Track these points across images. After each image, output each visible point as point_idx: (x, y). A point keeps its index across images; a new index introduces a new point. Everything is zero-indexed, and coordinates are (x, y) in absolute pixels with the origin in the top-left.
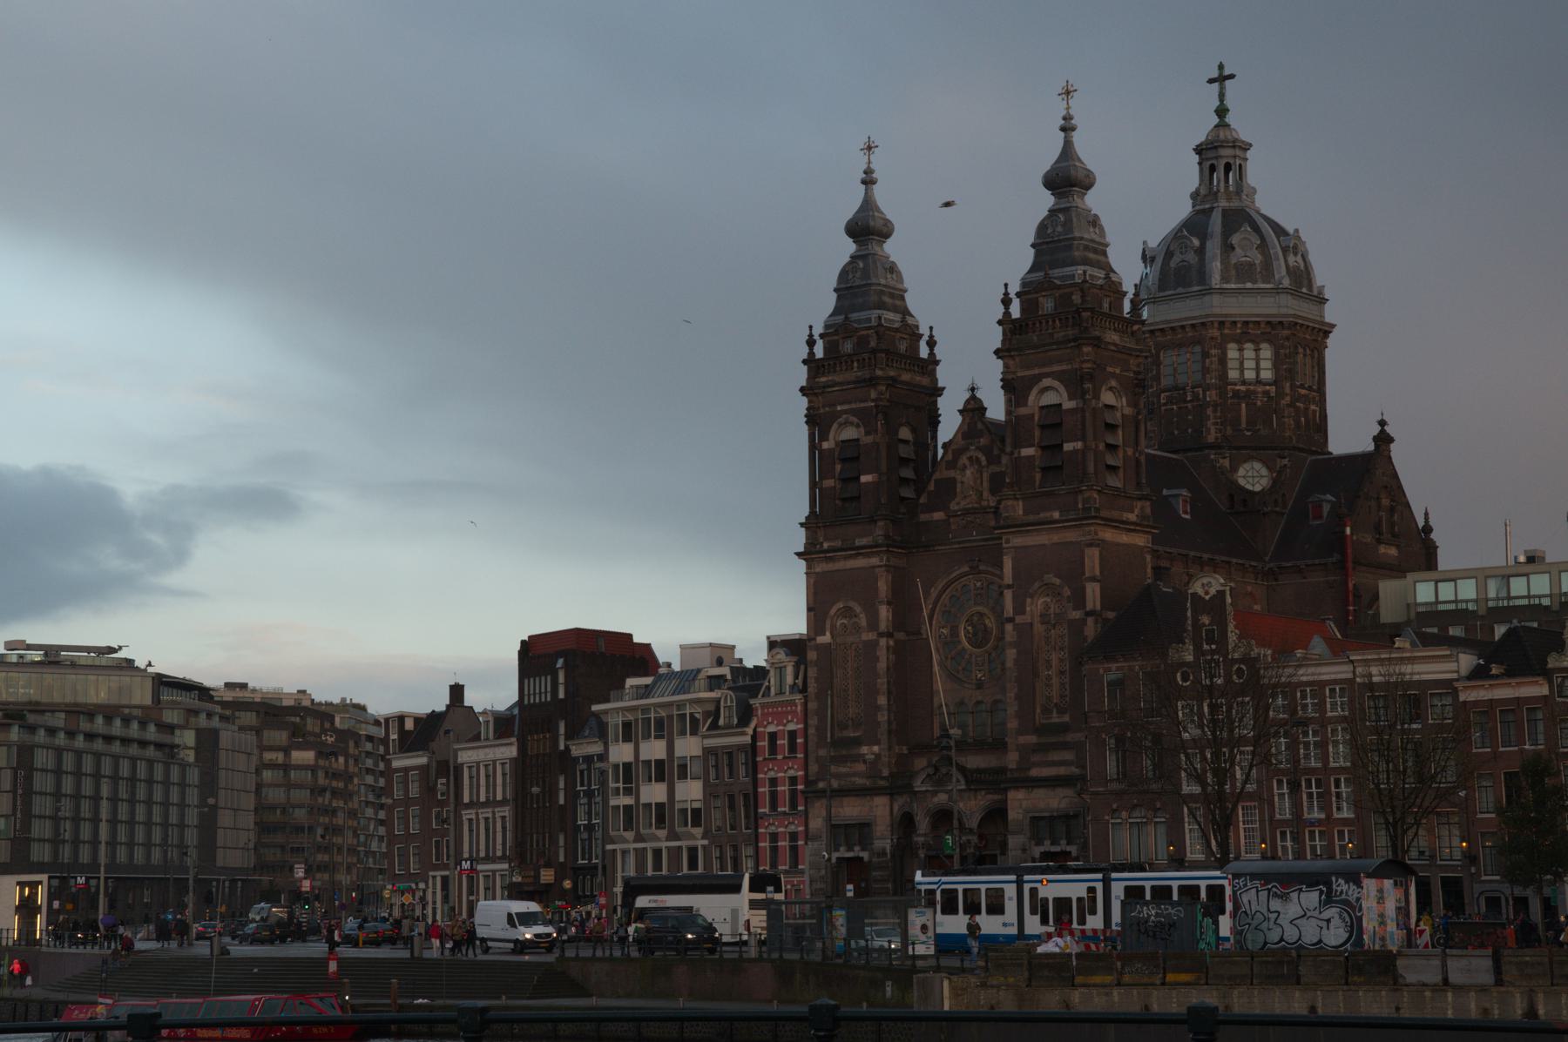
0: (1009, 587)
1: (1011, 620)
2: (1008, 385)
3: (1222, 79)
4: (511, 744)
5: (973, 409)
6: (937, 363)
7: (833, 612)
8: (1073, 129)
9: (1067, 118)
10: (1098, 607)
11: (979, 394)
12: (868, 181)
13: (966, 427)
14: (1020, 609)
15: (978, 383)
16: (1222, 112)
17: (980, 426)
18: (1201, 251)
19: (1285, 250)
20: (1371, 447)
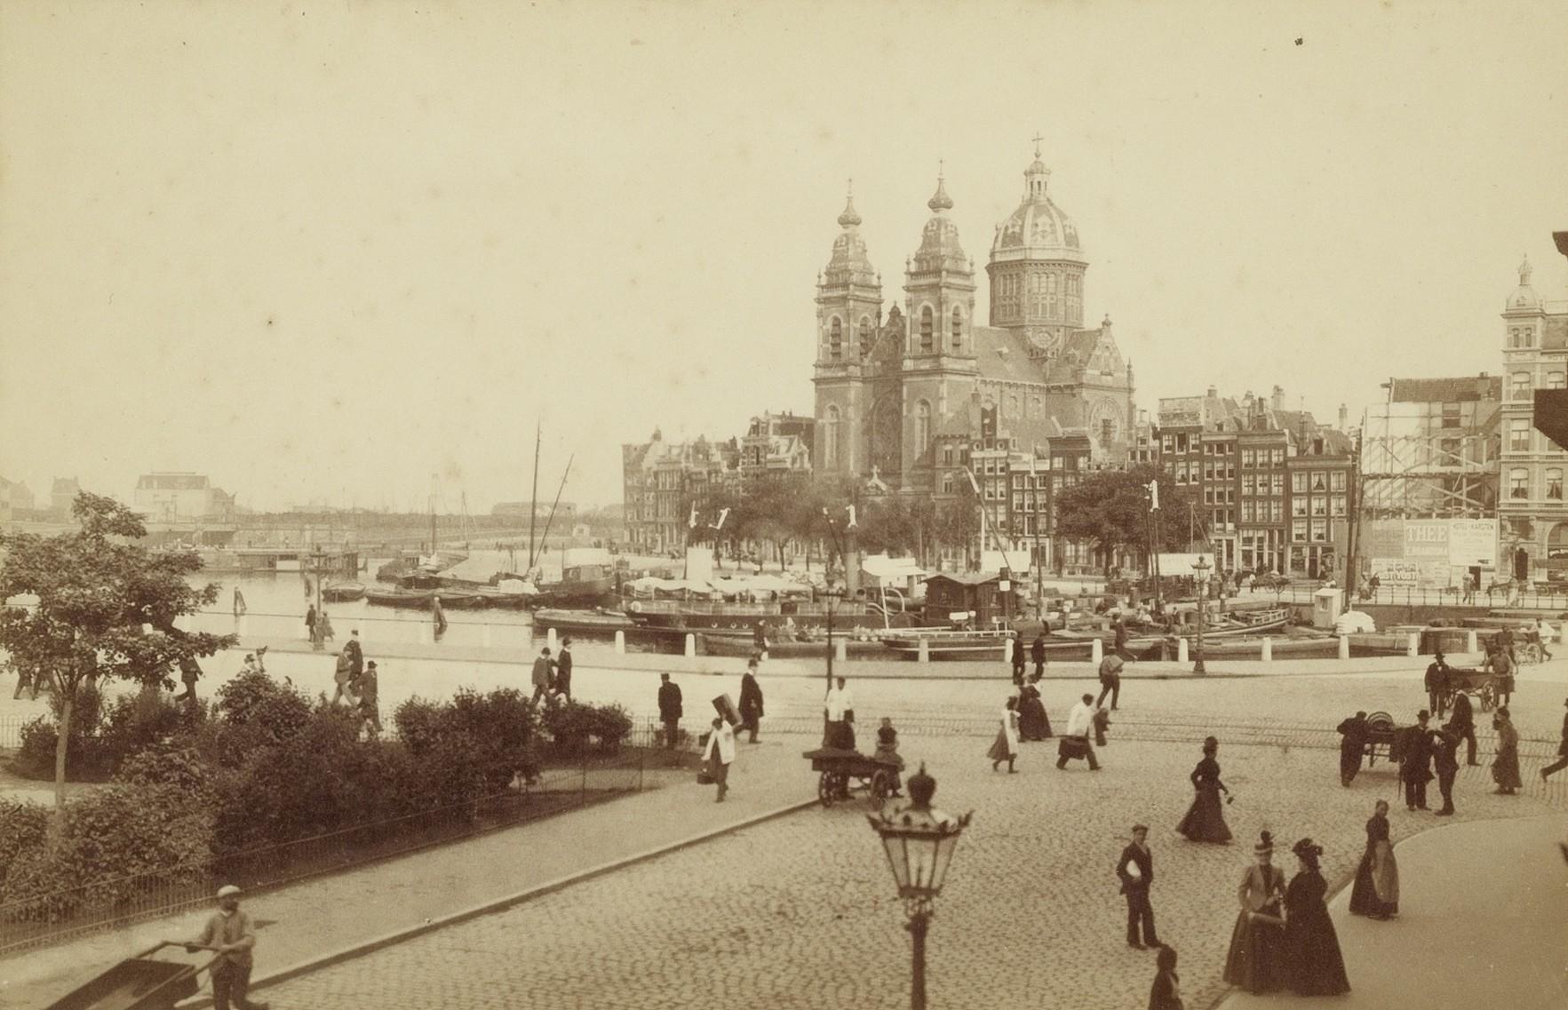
2: (909, 304)
6: (880, 287)
10: (945, 411)
11: (898, 305)
12: (850, 199)
14: (909, 411)
16: (1037, 156)
18: (1022, 227)
19: (1064, 227)
20: (1101, 326)
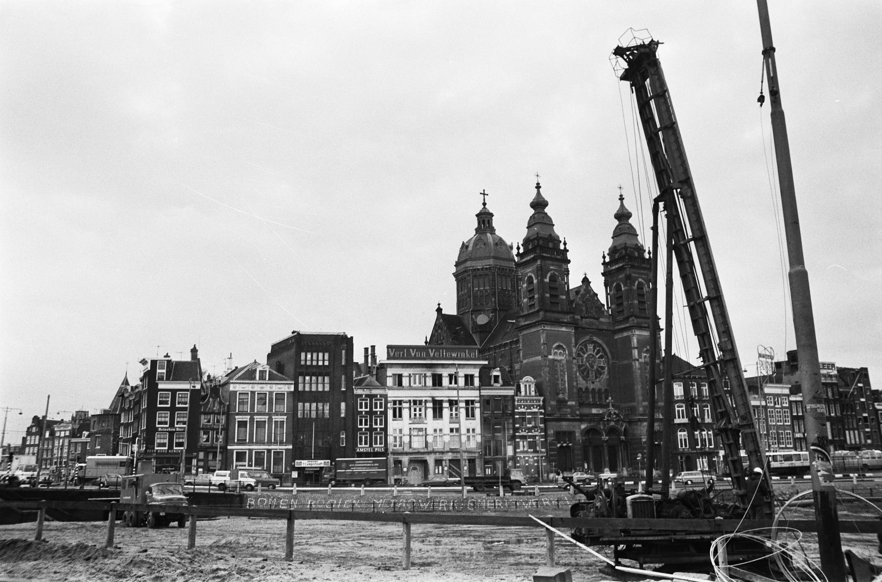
0: (637, 348)
1: (638, 360)
4: (292, 384)
5: (586, 281)
7: (555, 346)
8: (623, 199)
9: (621, 196)
11: (588, 277)
12: (538, 187)
13: (584, 287)
15: (587, 273)
16: (484, 204)
17: (589, 288)
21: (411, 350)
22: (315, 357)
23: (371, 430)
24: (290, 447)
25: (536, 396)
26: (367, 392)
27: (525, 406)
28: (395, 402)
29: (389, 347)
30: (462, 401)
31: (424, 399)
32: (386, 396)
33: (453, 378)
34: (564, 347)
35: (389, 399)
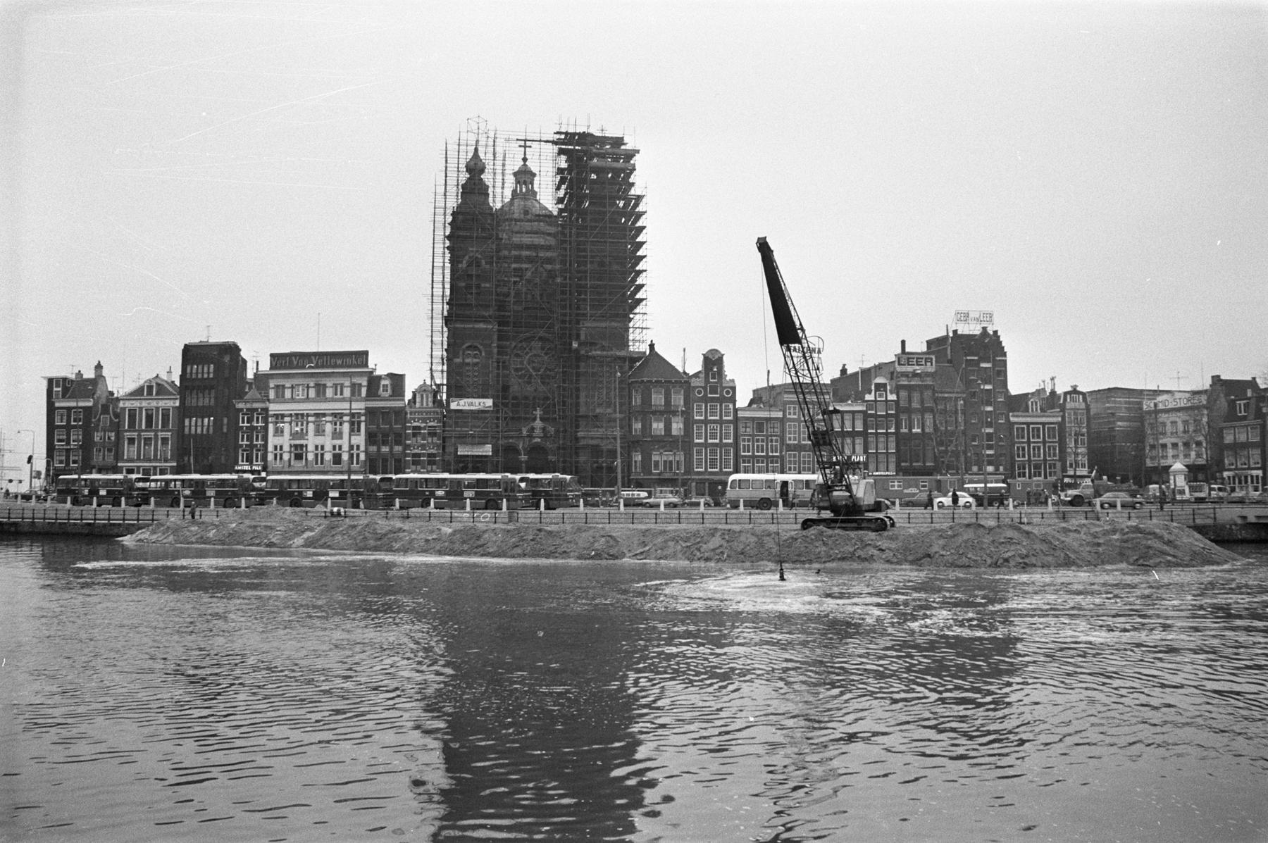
3: (525, 147)
7: (464, 347)
16: (525, 160)
21: (293, 358)
22: (200, 370)
23: (251, 446)
24: (175, 464)
25: (434, 407)
26: (248, 406)
27: (419, 419)
28: (277, 416)
29: (272, 356)
30: (346, 415)
31: (305, 412)
32: (266, 410)
33: (338, 388)
34: (481, 347)
35: (270, 413)
